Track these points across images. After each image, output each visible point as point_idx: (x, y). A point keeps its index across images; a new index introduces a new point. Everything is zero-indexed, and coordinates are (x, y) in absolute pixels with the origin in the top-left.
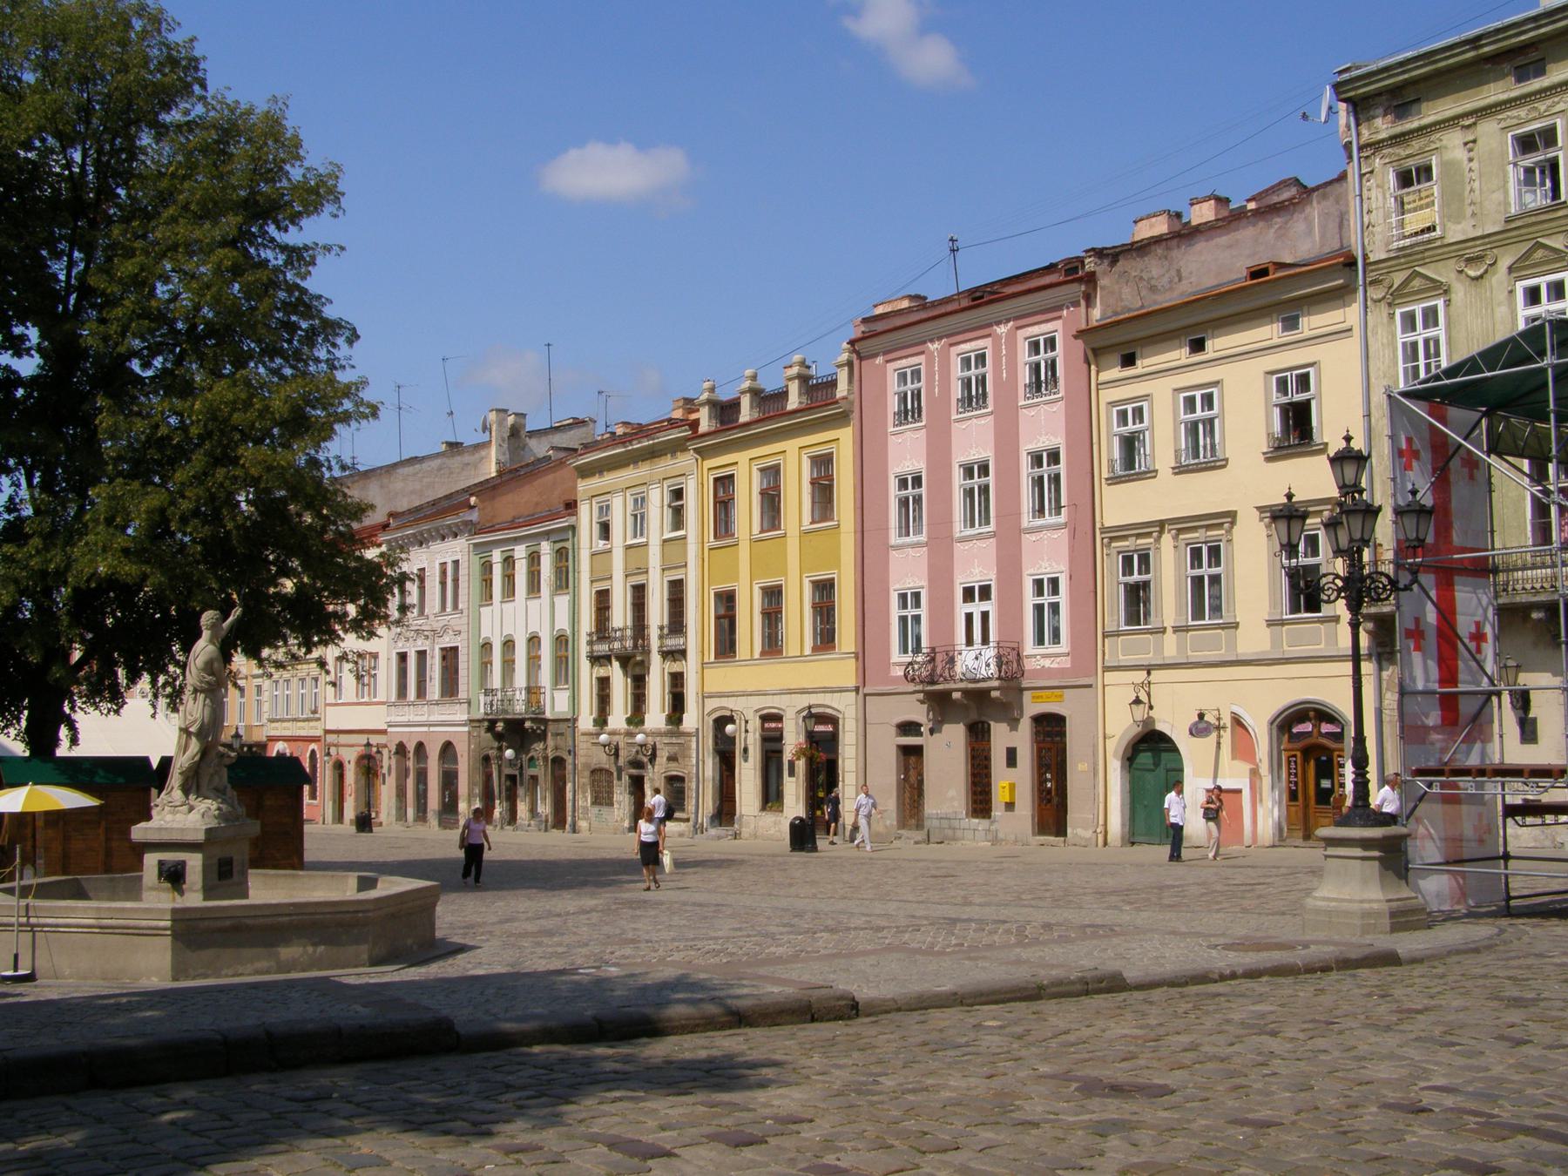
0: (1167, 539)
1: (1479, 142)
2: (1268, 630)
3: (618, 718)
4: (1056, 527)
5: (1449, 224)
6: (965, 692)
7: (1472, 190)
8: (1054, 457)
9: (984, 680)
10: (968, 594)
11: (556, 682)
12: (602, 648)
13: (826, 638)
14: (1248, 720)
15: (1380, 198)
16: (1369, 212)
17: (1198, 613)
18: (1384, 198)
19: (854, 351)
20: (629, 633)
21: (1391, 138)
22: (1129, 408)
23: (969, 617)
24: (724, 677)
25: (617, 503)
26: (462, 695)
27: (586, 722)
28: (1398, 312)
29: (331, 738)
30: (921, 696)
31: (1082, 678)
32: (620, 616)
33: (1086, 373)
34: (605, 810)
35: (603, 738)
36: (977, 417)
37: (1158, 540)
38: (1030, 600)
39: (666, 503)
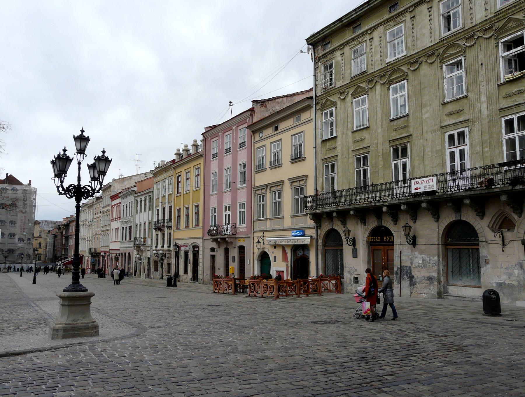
1: (345, 54)
3: (159, 247)
7: (342, 70)
11: (149, 236)
16: (317, 80)
21: (323, 55)
28: (324, 112)
29: (111, 252)
30: (212, 240)
37: (266, 190)
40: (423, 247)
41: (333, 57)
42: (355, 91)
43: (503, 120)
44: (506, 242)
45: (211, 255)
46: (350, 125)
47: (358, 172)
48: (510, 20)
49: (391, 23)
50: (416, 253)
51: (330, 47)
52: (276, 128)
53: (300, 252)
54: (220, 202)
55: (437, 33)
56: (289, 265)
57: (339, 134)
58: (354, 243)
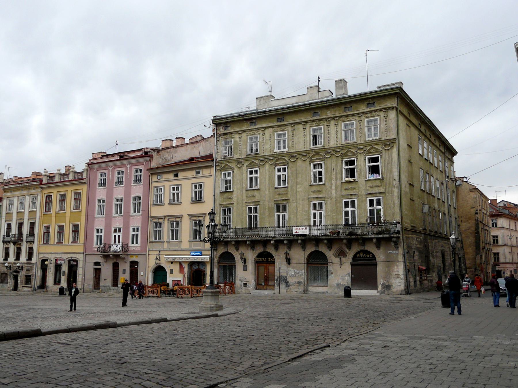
1: (242, 137)
2: (188, 243)
3: (12, 259)
4: (139, 216)
5: (235, 155)
6: (113, 255)
7: (240, 148)
8: (139, 198)
9: (118, 252)
10: (115, 231)
12: (7, 239)
13: (75, 240)
16: (218, 149)
18: (221, 147)
20: (17, 236)
21: (224, 133)
22: (159, 188)
23: (115, 236)
24: (45, 249)
25: (16, 200)
28: (222, 173)
30: (101, 256)
31: (144, 253)
32: (14, 230)
35: (6, 264)
37: (164, 220)
38: (131, 232)
39: (31, 201)
40: (295, 265)
41: (232, 137)
42: (250, 164)
43: (343, 200)
44: (342, 263)
45: (94, 268)
46: (244, 185)
47: (250, 217)
48: (349, 151)
49: (278, 128)
50: (290, 268)
51: (230, 130)
52: (176, 175)
53: (195, 267)
54: (108, 225)
55: (308, 144)
56: (186, 276)
57: (235, 190)
58: (244, 261)
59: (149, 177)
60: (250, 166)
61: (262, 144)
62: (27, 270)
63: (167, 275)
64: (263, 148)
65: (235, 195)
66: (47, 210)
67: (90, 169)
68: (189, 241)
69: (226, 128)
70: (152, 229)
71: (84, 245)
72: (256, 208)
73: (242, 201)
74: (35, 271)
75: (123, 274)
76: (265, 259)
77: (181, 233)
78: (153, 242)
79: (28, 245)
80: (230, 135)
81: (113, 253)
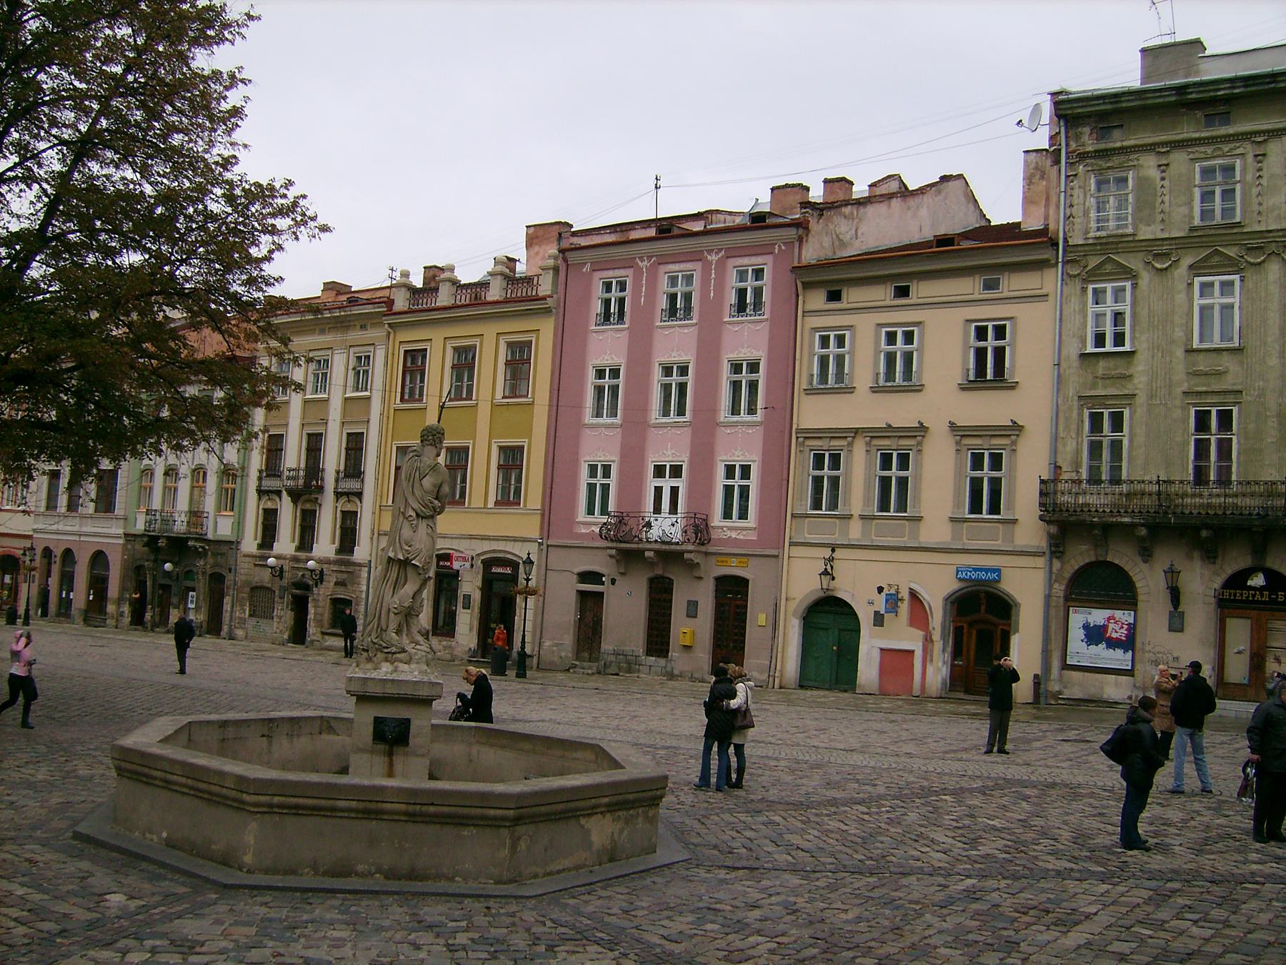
0: (859, 447)
1: (1171, 167)
3: (285, 544)
5: (1141, 226)
7: (1163, 202)
10: (659, 471)
12: (269, 484)
13: (509, 497)
14: (925, 595)
15: (1082, 197)
16: (1071, 206)
17: (884, 506)
18: (1085, 196)
19: (565, 260)
20: (302, 473)
21: (1095, 151)
22: (832, 334)
23: (658, 491)
26: (119, 509)
27: (250, 544)
32: (293, 457)
33: (794, 300)
34: (263, 622)
36: (680, 326)
39: (351, 367)
46: (1179, 334)
47: (1201, 448)
51: (1118, 140)
52: (903, 292)
54: (633, 452)
57: (1142, 346)
58: (1175, 595)
59: (794, 296)
60: (1204, 268)
61: (1255, 191)
62: (336, 584)
63: (859, 631)
64: (1260, 204)
65: (1140, 368)
66: (406, 397)
67: (568, 265)
68: (953, 520)
69: (1103, 132)
70: (801, 473)
71: (543, 515)
72: (1225, 419)
73: (1170, 387)
74: (364, 588)
75: (688, 616)
76: (1262, 596)
77: (917, 489)
78: (807, 516)
79: (339, 505)
80: (1122, 158)
81: (657, 546)
